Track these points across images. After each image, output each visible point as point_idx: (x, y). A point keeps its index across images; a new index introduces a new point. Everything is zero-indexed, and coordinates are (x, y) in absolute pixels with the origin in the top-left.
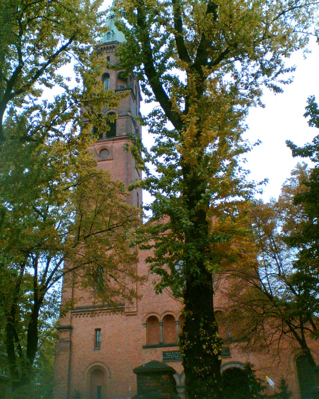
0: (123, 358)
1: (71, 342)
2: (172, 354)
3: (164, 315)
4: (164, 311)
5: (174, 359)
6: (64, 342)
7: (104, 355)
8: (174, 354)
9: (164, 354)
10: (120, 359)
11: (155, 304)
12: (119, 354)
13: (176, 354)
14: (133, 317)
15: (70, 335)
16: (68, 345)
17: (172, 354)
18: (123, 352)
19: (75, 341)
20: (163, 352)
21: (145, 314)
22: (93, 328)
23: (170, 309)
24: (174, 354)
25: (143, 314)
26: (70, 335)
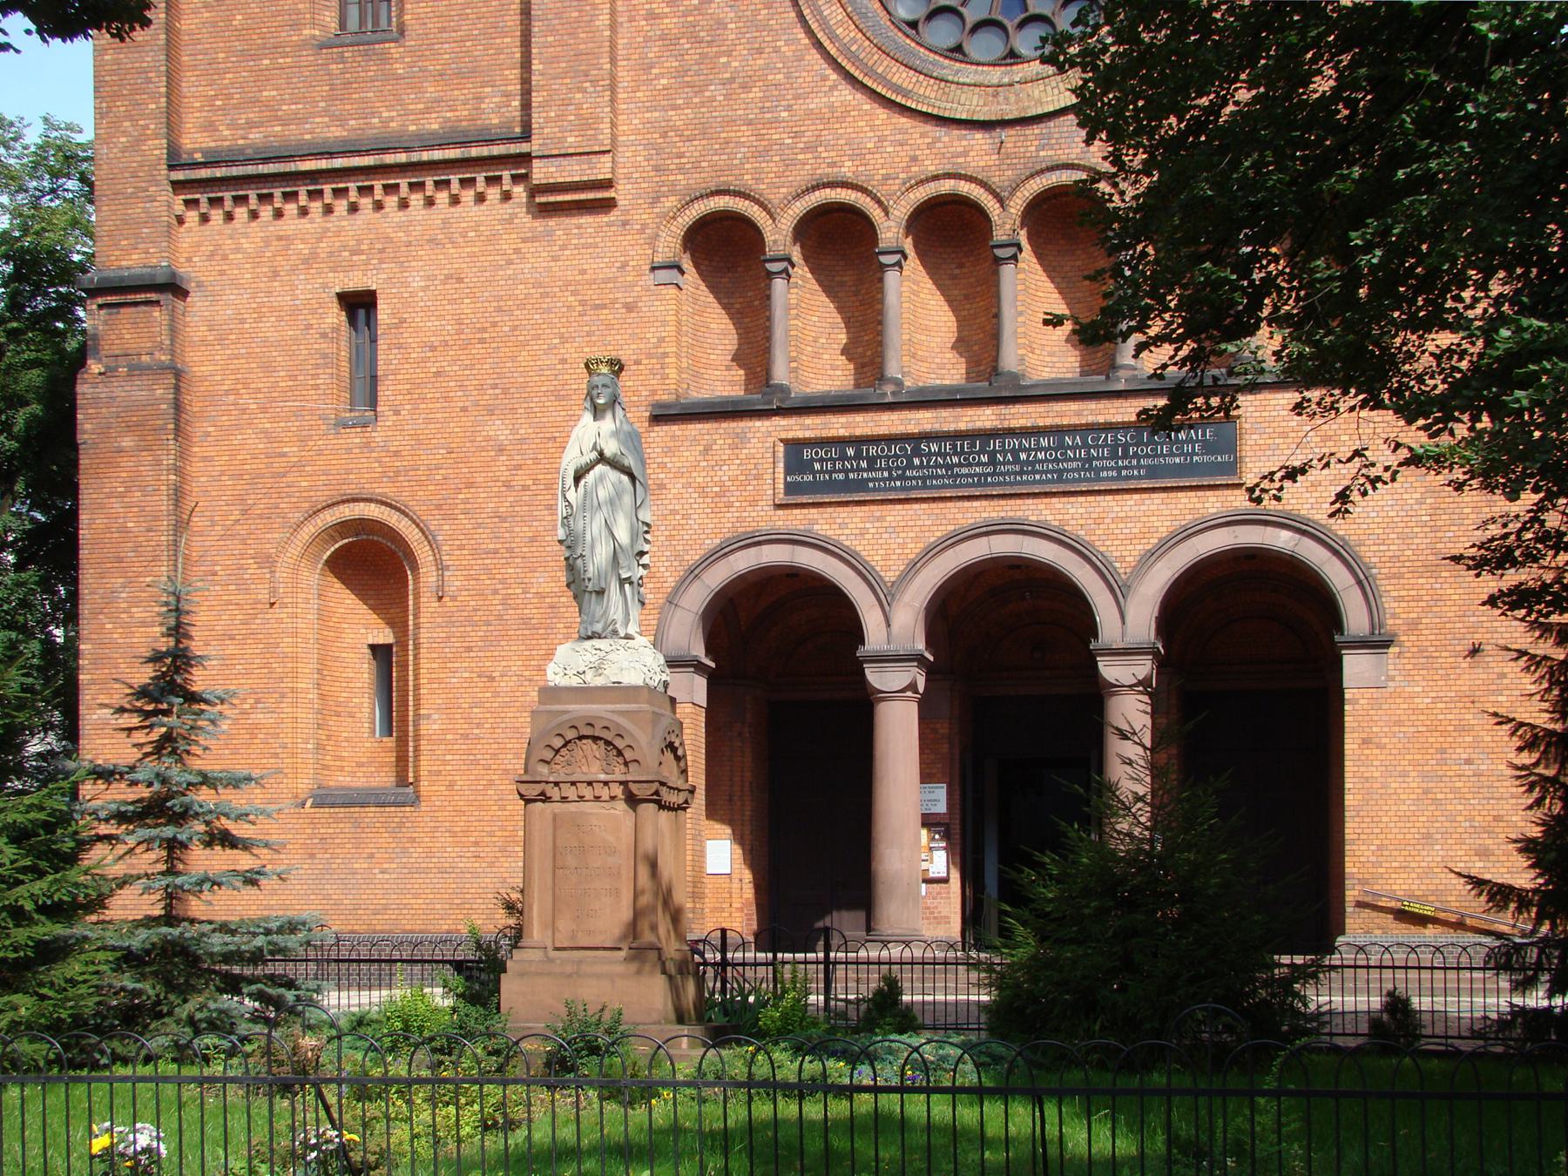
0: (520, 479)
1: (178, 374)
2: (843, 457)
3: (800, 207)
4: (801, 176)
5: (861, 485)
6: (137, 370)
7: (396, 454)
8: (858, 456)
9: (794, 447)
10: (508, 485)
11: (745, 134)
12: (501, 450)
13: (872, 461)
14: (586, 220)
15: (173, 332)
16: (162, 391)
17: (843, 457)
18: (522, 441)
19: (202, 364)
20: (785, 441)
21: (671, 202)
22: (325, 286)
23: (847, 170)
24: (858, 456)
25: (656, 200)
26: (173, 332)
